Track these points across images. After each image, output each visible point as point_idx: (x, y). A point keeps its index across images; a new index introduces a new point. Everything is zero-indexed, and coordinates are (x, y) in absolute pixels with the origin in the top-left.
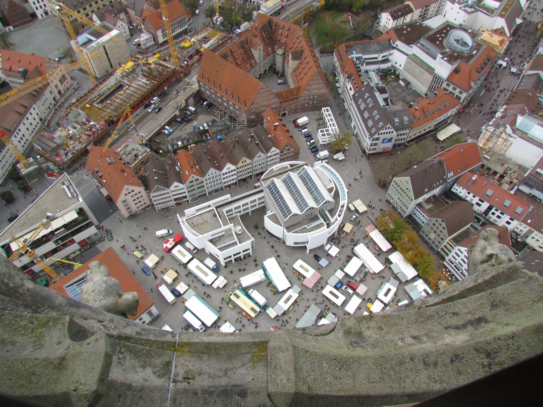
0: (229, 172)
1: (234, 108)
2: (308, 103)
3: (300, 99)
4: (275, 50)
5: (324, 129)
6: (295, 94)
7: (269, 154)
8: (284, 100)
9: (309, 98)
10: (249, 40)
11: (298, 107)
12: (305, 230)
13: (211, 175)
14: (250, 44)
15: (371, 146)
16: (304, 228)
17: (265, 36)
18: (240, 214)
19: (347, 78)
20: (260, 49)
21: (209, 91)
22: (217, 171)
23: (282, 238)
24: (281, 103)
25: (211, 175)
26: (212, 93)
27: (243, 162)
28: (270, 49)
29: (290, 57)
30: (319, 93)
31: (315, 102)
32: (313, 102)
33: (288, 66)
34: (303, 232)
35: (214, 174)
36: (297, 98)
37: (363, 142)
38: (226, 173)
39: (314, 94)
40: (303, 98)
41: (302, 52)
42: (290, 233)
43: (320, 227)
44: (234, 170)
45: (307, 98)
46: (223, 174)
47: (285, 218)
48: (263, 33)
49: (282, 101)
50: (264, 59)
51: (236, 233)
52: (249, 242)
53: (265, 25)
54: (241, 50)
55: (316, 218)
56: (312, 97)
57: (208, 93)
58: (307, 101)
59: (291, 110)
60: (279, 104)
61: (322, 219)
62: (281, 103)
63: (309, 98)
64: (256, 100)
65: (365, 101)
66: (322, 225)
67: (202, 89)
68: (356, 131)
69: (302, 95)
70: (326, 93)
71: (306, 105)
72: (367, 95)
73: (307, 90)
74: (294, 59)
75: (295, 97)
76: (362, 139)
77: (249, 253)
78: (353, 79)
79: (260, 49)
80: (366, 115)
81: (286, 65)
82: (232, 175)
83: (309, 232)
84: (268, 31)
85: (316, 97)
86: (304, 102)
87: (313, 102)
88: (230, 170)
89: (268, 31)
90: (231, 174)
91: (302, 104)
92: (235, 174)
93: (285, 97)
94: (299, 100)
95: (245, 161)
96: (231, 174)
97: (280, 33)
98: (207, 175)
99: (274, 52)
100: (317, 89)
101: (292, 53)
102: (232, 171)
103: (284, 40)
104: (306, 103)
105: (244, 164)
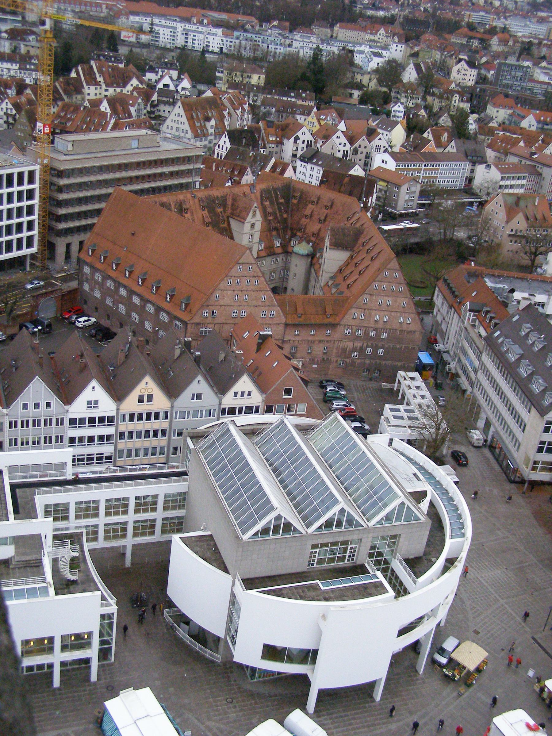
0: (92, 420)
1: (157, 322)
2: (362, 351)
3: (340, 329)
4: (290, 250)
5: (401, 407)
6: (329, 311)
7: (229, 401)
8: (297, 321)
9: (366, 334)
10: (229, 202)
11: (333, 358)
12: (312, 593)
13: (31, 406)
14: (229, 211)
15: (540, 450)
16: (309, 587)
17: (269, 210)
18: (94, 545)
19: (470, 311)
20: (253, 226)
21: (102, 286)
22: (55, 400)
23: (222, 636)
24: (287, 325)
25: (31, 406)
26: (106, 292)
27: (141, 400)
28: (277, 243)
29: (327, 243)
30: (396, 326)
31: (381, 352)
32: (375, 348)
33: (317, 277)
34: (302, 598)
35: (43, 405)
36: (333, 326)
37: (513, 450)
38: (82, 421)
39: (380, 325)
40: (348, 332)
41: (358, 233)
42: (253, 592)
43: (371, 595)
44: (111, 420)
45: (360, 333)
46: (73, 422)
47: (244, 533)
48: (267, 203)
49: (290, 321)
50: (259, 257)
51: (55, 561)
52: (99, 593)
53: (275, 190)
54: (206, 212)
55: (360, 570)
56: (373, 334)
57: (97, 294)
58: (358, 344)
59: (312, 361)
60: (281, 328)
61: (379, 574)
62: (287, 325)
63: (366, 334)
64: (218, 294)
65: (521, 341)
66: (378, 589)
67: (86, 287)
68: (492, 429)
69: (348, 319)
70: (412, 328)
71: (355, 355)
72: (526, 328)
73: (364, 308)
74: (337, 245)
75: (327, 321)
76: (510, 446)
77: (87, 661)
78: (487, 312)
79: (253, 226)
80: (523, 371)
81: (312, 283)
82: (101, 438)
83: (327, 600)
84: (279, 204)
85: (384, 336)
86: (350, 345)
87: (375, 348)
88: (96, 413)
89: (279, 204)
90: (97, 431)
91: (344, 350)
92: (109, 437)
93: (300, 311)
94: (337, 336)
95: (150, 398)
96: (97, 431)
97: (308, 212)
98: (19, 402)
99: (286, 251)
100: (389, 309)
101: (332, 230)
102: (102, 420)
103: (314, 227)
104: (354, 349)
105: (145, 408)
